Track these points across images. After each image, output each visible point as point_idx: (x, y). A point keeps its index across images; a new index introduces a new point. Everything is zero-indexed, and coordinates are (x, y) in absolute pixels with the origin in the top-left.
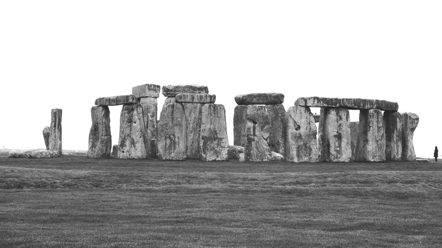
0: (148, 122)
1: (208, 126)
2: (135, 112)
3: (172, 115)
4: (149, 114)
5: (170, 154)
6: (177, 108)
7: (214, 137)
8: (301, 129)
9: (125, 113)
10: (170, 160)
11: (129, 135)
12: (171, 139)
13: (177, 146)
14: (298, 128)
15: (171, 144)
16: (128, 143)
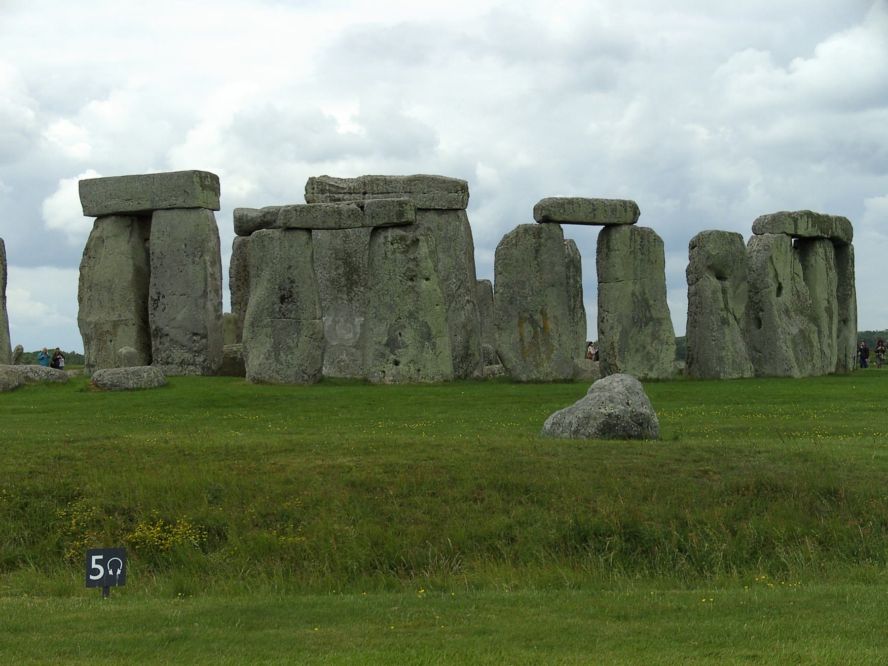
0: (206, 279)
1: (630, 287)
2: (424, 249)
3: (536, 257)
4: (207, 258)
5: (537, 366)
6: (550, 238)
7: (645, 316)
8: (783, 292)
9: (394, 252)
10: (537, 382)
11: (411, 315)
12: (533, 323)
13: (556, 343)
14: (780, 289)
15: (535, 337)
16: (409, 336)
